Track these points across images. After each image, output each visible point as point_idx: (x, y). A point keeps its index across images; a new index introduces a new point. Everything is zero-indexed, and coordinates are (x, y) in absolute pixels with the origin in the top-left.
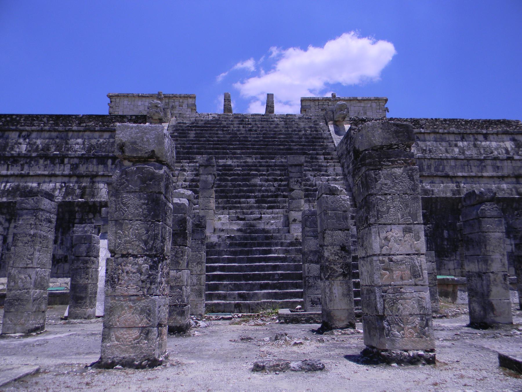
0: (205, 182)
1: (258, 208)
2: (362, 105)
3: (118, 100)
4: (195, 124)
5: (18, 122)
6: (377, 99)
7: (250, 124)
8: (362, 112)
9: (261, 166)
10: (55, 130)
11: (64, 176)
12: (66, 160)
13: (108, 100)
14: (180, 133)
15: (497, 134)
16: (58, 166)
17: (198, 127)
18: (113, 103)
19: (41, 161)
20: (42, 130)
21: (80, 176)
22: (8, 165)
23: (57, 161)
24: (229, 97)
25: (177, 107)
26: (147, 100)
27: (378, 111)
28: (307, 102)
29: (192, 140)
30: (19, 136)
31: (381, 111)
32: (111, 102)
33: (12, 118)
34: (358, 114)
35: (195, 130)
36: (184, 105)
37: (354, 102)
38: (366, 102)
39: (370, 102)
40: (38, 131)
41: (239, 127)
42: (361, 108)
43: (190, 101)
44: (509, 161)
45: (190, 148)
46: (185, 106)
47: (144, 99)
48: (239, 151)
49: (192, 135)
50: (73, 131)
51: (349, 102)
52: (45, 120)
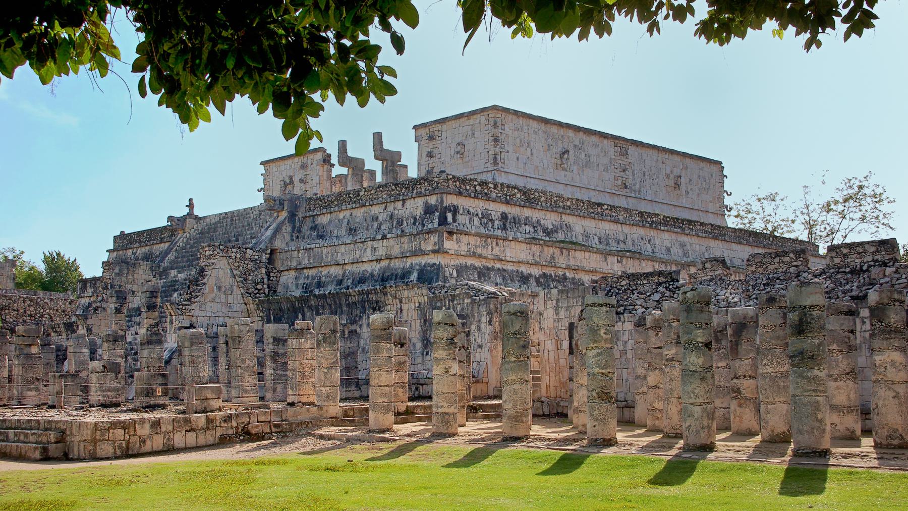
2: (471, 122)
8: (470, 133)
13: (262, 170)
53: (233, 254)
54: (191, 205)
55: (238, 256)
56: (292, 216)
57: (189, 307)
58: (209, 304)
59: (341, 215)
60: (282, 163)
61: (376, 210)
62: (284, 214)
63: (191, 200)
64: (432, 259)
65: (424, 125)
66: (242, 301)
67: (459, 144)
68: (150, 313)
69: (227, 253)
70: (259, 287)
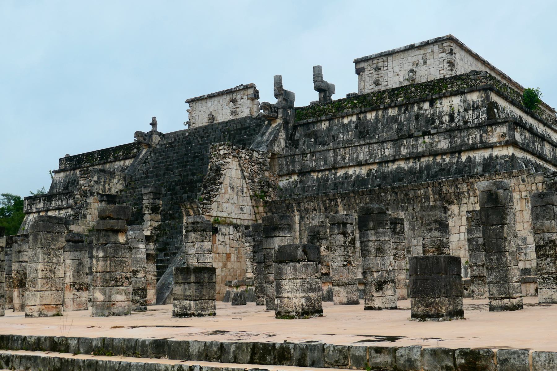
2: (422, 52)
6: (438, 41)
8: (422, 61)
27: (441, 55)
31: (444, 54)
33: (79, 157)
39: (431, 46)
42: (421, 57)
43: (251, 91)
44: (426, 137)
46: (245, 97)
47: (213, 99)
51: (406, 52)
53: (243, 155)
54: (154, 124)
55: (247, 157)
56: (286, 122)
57: (209, 206)
58: (225, 204)
59: (346, 121)
61: (392, 112)
62: (279, 121)
63: (154, 118)
64: (498, 152)
65: (366, 60)
66: (250, 204)
67: (412, 71)
68: (153, 216)
69: (238, 153)
70: (265, 189)
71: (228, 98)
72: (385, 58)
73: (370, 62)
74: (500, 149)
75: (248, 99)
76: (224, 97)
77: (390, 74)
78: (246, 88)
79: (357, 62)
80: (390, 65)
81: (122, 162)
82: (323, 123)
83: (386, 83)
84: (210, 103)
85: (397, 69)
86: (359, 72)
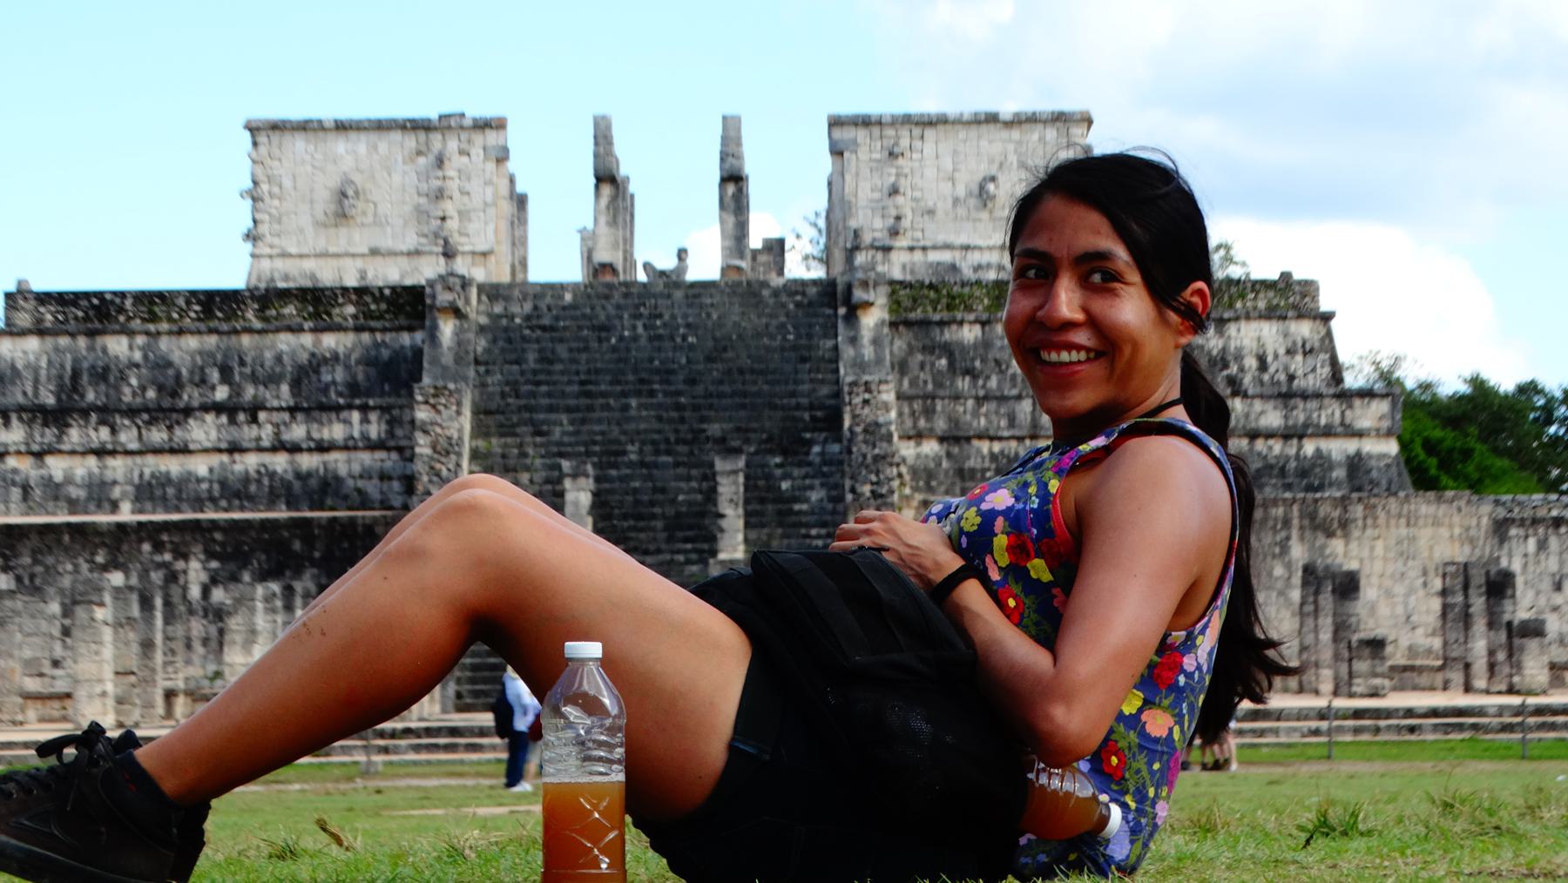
0: (576, 504)
1: (670, 539)
2: (1015, 134)
3: (275, 137)
4: (534, 322)
5: (121, 310)
7: (660, 316)
9: (678, 442)
10: (211, 331)
11: (260, 450)
12: (262, 416)
14: (503, 350)
15: (1248, 317)
16: (246, 428)
17: (544, 328)
18: (263, 149)
19: (210, 418)
20: (181, 332)
21: (294, 449)
22: (139, 428)
23: (241, 417)
24: (609, 127)
25: (456, 157)
26: (363, 137)
28: (846, 129)
29: (535, 372)
30: (131, 348)
32: (255, 144)
34: (1001, 165)
35: (538, 341)
36: (473, 152)
37: (992, 127)
38: (1026, 127)
39: (1040, 126)
40: (170, 333)
41: (634, 328)
42: (1011, 147)
43: (492, 137)
45: (533, 395)
46: (477, 152)
47: (353, 135)
48: (634, 402)
49: (531, 357)
50: (250, 331)
51: (974, 127)
52: (181, 302)
60: (331, 136)
64: (1371, 446)
65: (865, 122)
67: (993, 179)
71: (411, 141)
72: (917, 131)
73: (876, 131)
74: (1374, 440)
75: (486, 157)
76: (396, 136)
77: (930, 173)
78: (483, 125)
79: (835, 123)
80: (929, 148)
81: (307, 339)
82: (966, 328)
83: (918, 194)
84: (340, 145)
85: (948, 164)
86: (837, 152)
